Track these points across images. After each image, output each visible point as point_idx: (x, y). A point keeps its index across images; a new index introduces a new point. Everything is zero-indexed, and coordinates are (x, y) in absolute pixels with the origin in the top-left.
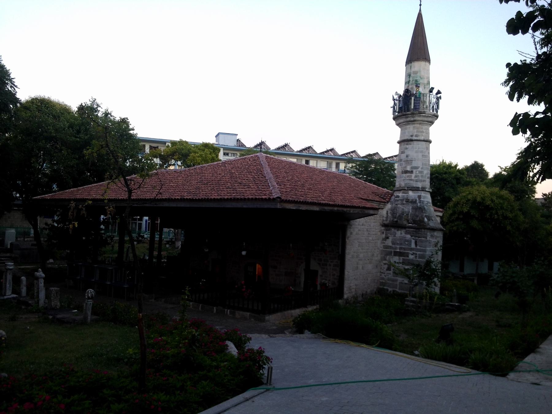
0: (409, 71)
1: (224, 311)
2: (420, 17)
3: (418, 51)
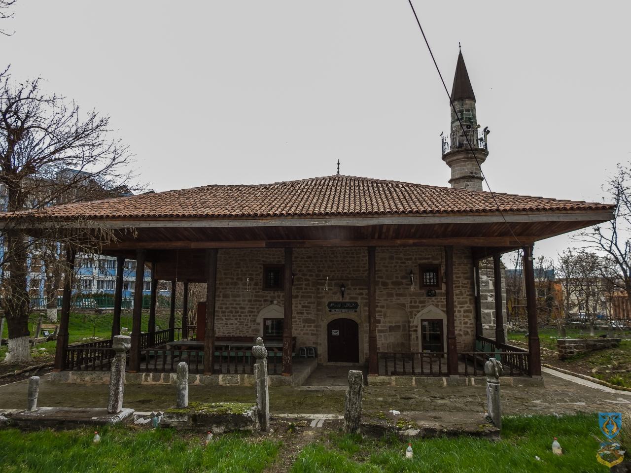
0: (458, 108)
1: (465, 381)
2: (461, 57)
3: (462, 92)
